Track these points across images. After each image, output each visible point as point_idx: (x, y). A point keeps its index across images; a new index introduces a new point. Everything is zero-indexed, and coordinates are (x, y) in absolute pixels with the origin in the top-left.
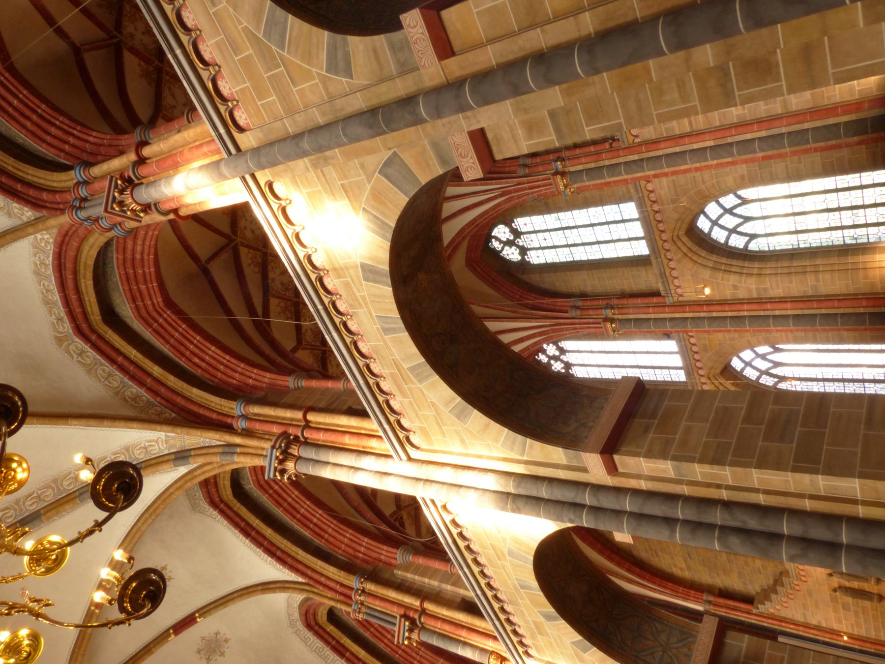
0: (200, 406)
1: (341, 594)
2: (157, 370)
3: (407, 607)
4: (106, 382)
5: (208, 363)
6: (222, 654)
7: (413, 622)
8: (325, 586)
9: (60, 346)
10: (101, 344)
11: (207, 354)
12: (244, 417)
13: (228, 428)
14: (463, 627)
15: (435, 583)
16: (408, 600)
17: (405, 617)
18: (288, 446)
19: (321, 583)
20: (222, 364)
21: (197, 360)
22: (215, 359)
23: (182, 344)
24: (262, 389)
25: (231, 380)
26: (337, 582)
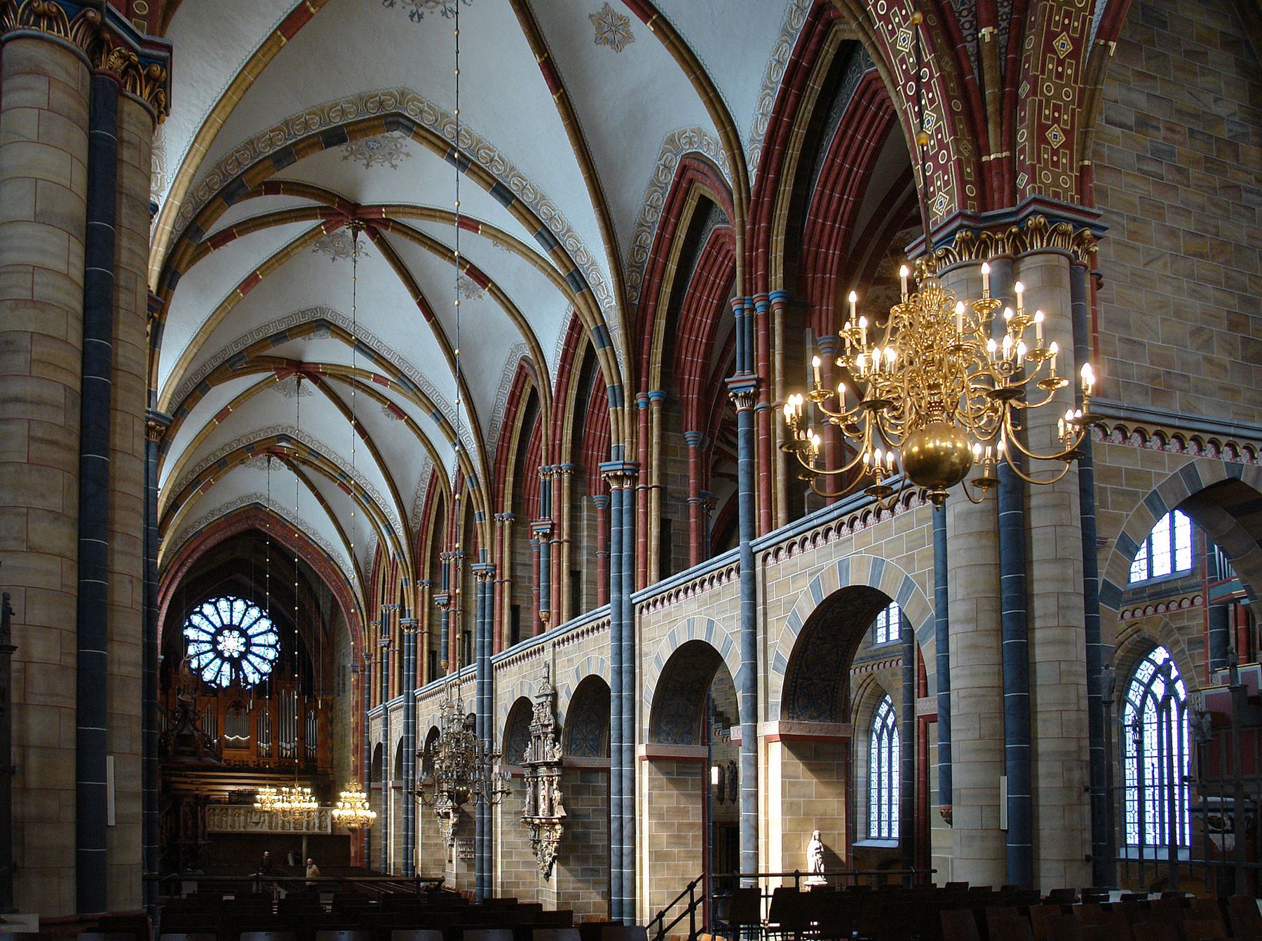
0: (651, 334)
1: (554, 445)
2: (672, 267)
3: (560, 525)
4: (647, 208)
5: (694, 319)
6: (468, 297)
7: (552, 534)
8: (555, 424)
9: (667, 143)
10: (680, 195)
11: (702, 317)
12: (648, 403)
13: (636, 387)
14: (559, 584)
15: (585, 543)
16: (565, 524)
17: (553, 525)
18: (628, 477)
19: (556, 421)
20: (697, 337)
21: (694, 306)
22: (700, 325)
23: (705, 285)
24: (682, 394)
25: (684, 352)
26: (561, 440)
